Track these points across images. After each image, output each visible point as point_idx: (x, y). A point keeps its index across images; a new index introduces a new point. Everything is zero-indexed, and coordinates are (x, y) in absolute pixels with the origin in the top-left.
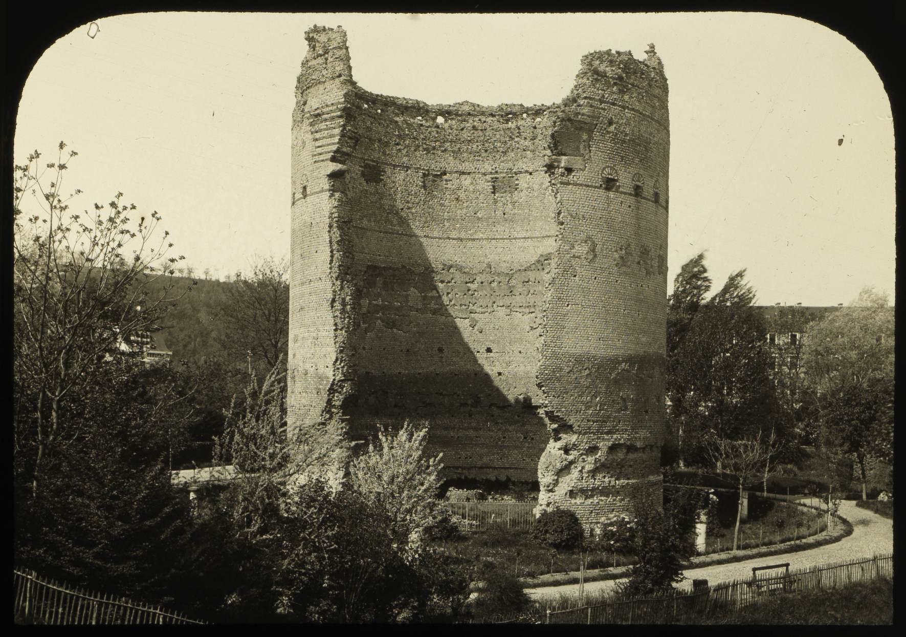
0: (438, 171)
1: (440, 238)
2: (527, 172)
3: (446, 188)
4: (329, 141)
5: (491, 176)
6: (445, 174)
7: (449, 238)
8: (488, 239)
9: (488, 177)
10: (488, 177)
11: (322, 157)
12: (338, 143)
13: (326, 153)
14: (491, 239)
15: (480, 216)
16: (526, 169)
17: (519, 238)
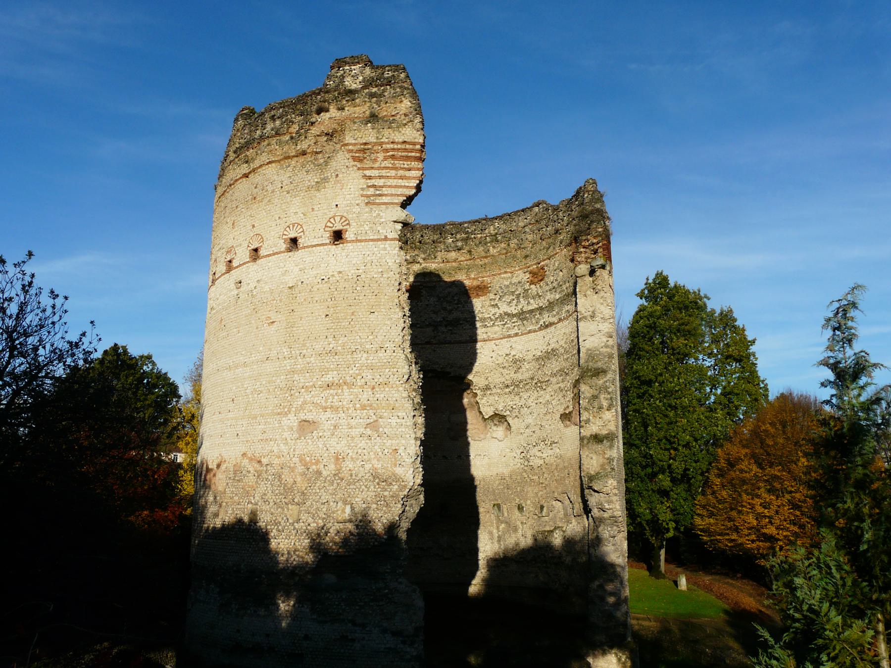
11: (385, 199)
13: (392, 195)
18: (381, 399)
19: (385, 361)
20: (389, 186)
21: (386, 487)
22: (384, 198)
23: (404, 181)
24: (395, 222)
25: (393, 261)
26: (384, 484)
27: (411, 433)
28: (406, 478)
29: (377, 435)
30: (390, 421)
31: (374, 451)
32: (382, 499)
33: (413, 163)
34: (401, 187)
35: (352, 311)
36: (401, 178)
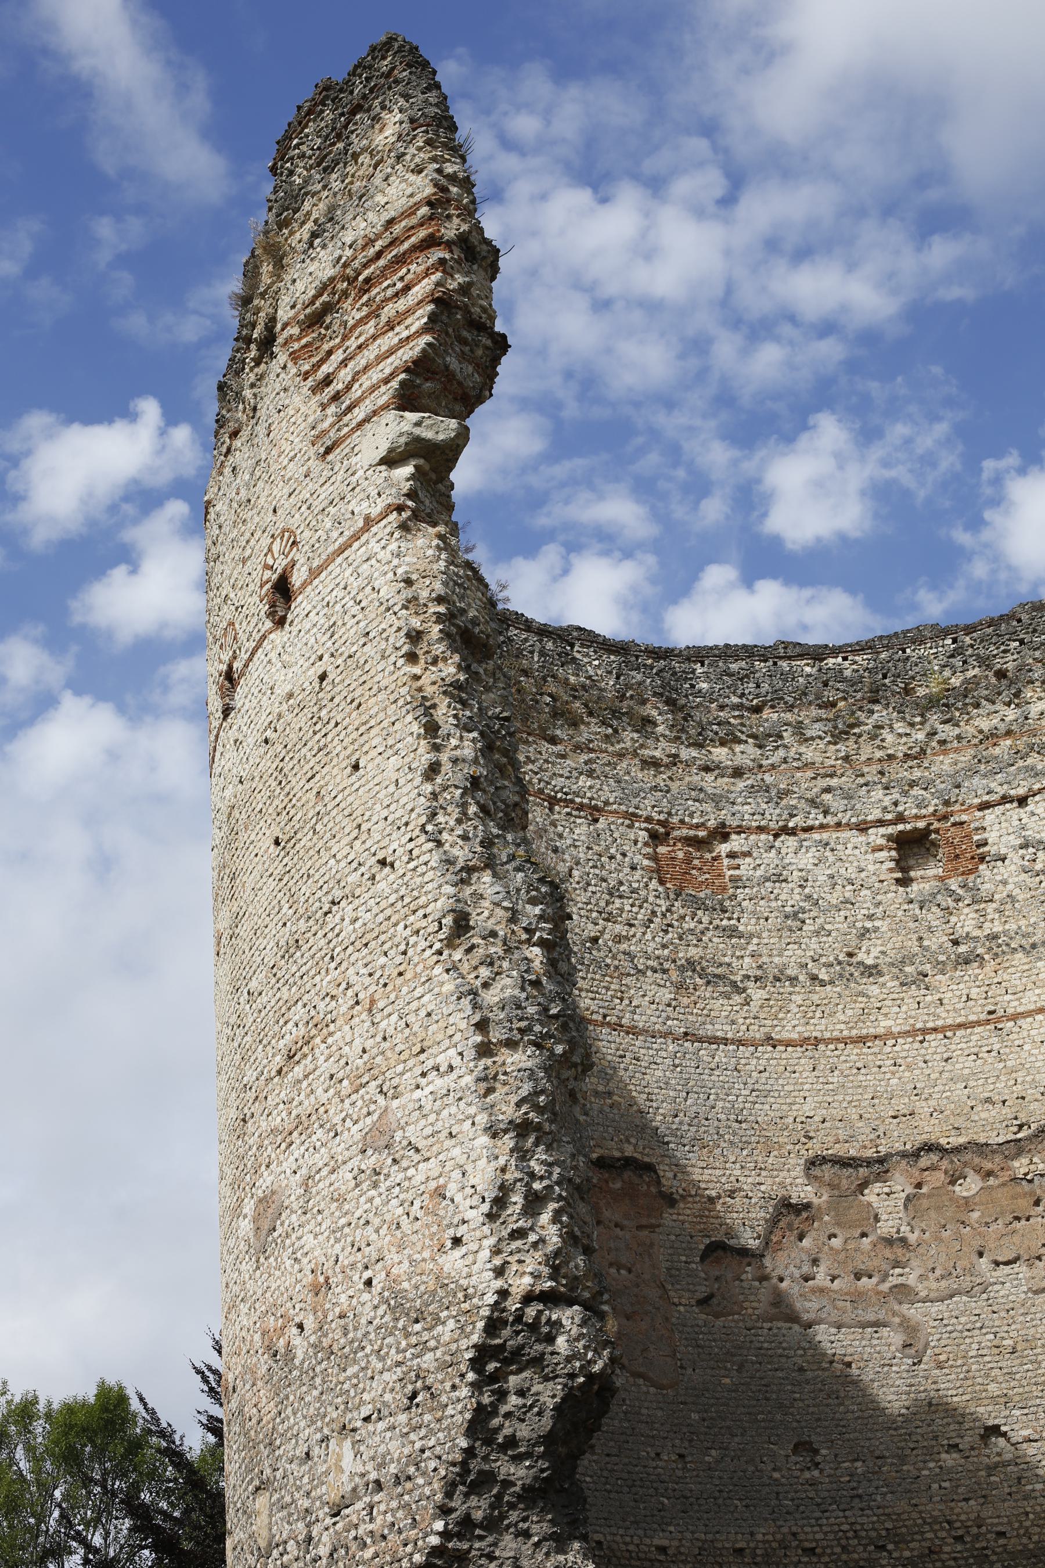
0: (697, 826)
1: (740, 1043)
2: (1005, 799)
3: (734, 879)
4: (390, 340)
5: (882, 830)
6: (725, 837)
7: (770, 1041)
8: (911, 1033)
9: (877, 836)
10: (877, 836)
12: (425, 330)
13: (374, 388)
14: (925, 1031)
15: (869, 962)
16: (1001, 791)
17: (1029, 1014)
18: (393, 1032)
19: (392, 899)
20: (366, 369)
21: (426, 1336)
22: (356, 410)
23: (397, 329)
24: (383, 461)
25: (390, 575)
26: (418, 1327)
27: (472, 1110)
28: (474, 1280)
29: (389, 1161)
30: (418, 1094)
31: (388, 1217)
32: (419, 1384)
33: (413, 267)
34: (391, 352)
35: (314, 791)
36: (390, 326)
